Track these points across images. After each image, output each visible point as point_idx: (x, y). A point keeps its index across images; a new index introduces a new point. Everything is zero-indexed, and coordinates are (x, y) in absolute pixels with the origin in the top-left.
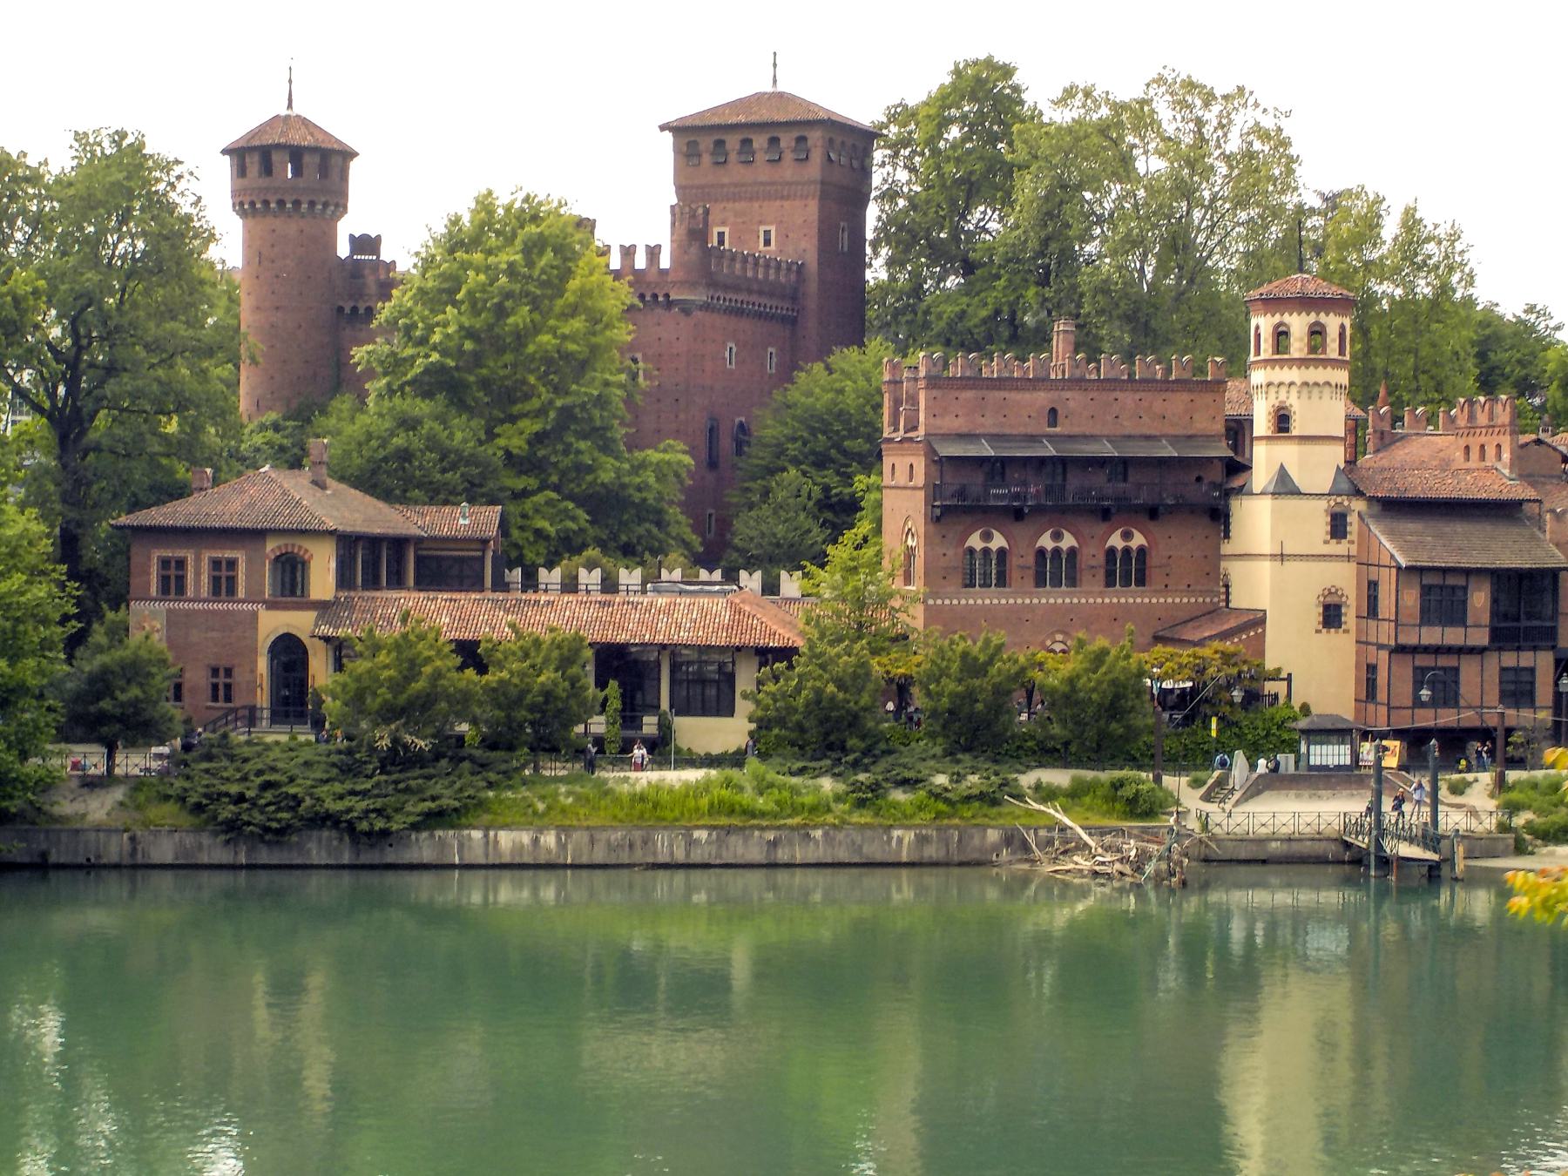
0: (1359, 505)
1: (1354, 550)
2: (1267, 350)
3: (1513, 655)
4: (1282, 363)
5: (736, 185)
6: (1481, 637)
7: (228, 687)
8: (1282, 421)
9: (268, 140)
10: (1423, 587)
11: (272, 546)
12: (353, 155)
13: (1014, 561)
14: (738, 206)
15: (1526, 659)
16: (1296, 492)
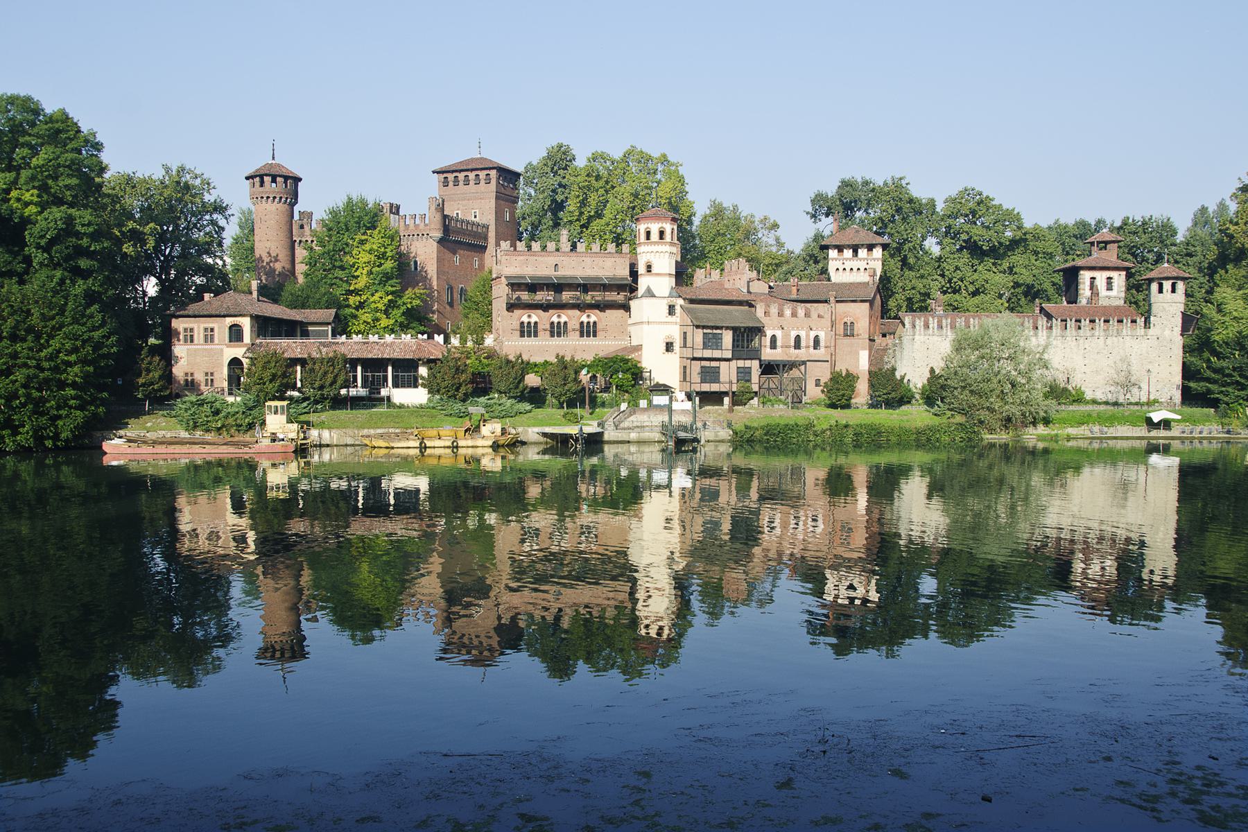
0: (680, 302)
1: (678, 320)
3: (743, 361)
4: (647, 244)
6: (729, 355)
7: (212, 380)
8: (649, 268)
9: (262, 172)
10: (704, 334)
11: (229, 321)
12: (300, 180)
13: (540, 327)
14: (464, 202)
15: (748, 363)
16: (653, 296)
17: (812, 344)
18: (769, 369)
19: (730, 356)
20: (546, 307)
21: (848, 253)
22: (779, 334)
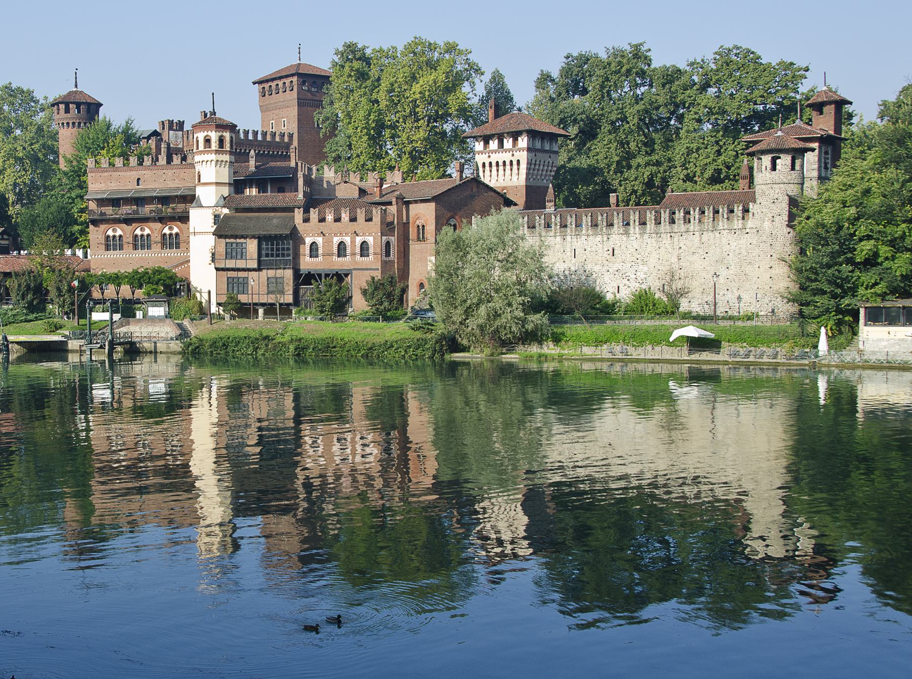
2: (201, 147)
3: (274, 271)
5: (275, 103)
6: (254, 265)
13: (125, 240)
14: (277, 111)
15: (280, 273)
17: (358, 250)
18: (303, 279)
19: (255, 266)
20: (128, 221)
21: (494, 144)
22: (319, 240)
